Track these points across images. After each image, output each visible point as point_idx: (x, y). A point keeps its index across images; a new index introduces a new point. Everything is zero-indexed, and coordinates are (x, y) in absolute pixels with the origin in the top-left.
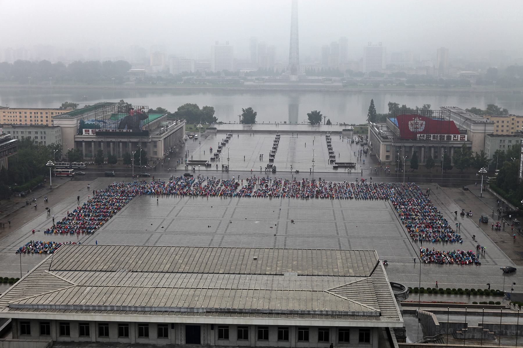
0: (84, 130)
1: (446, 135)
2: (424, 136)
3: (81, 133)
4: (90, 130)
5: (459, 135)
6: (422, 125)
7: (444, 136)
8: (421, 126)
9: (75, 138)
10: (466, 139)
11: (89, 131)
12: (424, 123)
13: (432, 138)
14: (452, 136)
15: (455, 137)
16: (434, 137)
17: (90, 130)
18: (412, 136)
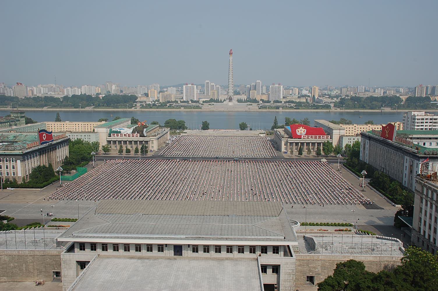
0: (112, 134)
1: (318, 136)
2: (305, 136)
3: (110, 136)
4: (116, 134)
5: (325, 136)
6: (304, 131)
7: (317, 136)
8: (304, 131)
9: (107, 139)
10: (329, 138)
11: (114, 135)
12: (306, 130)
13: (310, 137)
14: (321, 136)
15: (323, 137)
16: (311, 137)
17: (116, 134)
18: (300, 137)
